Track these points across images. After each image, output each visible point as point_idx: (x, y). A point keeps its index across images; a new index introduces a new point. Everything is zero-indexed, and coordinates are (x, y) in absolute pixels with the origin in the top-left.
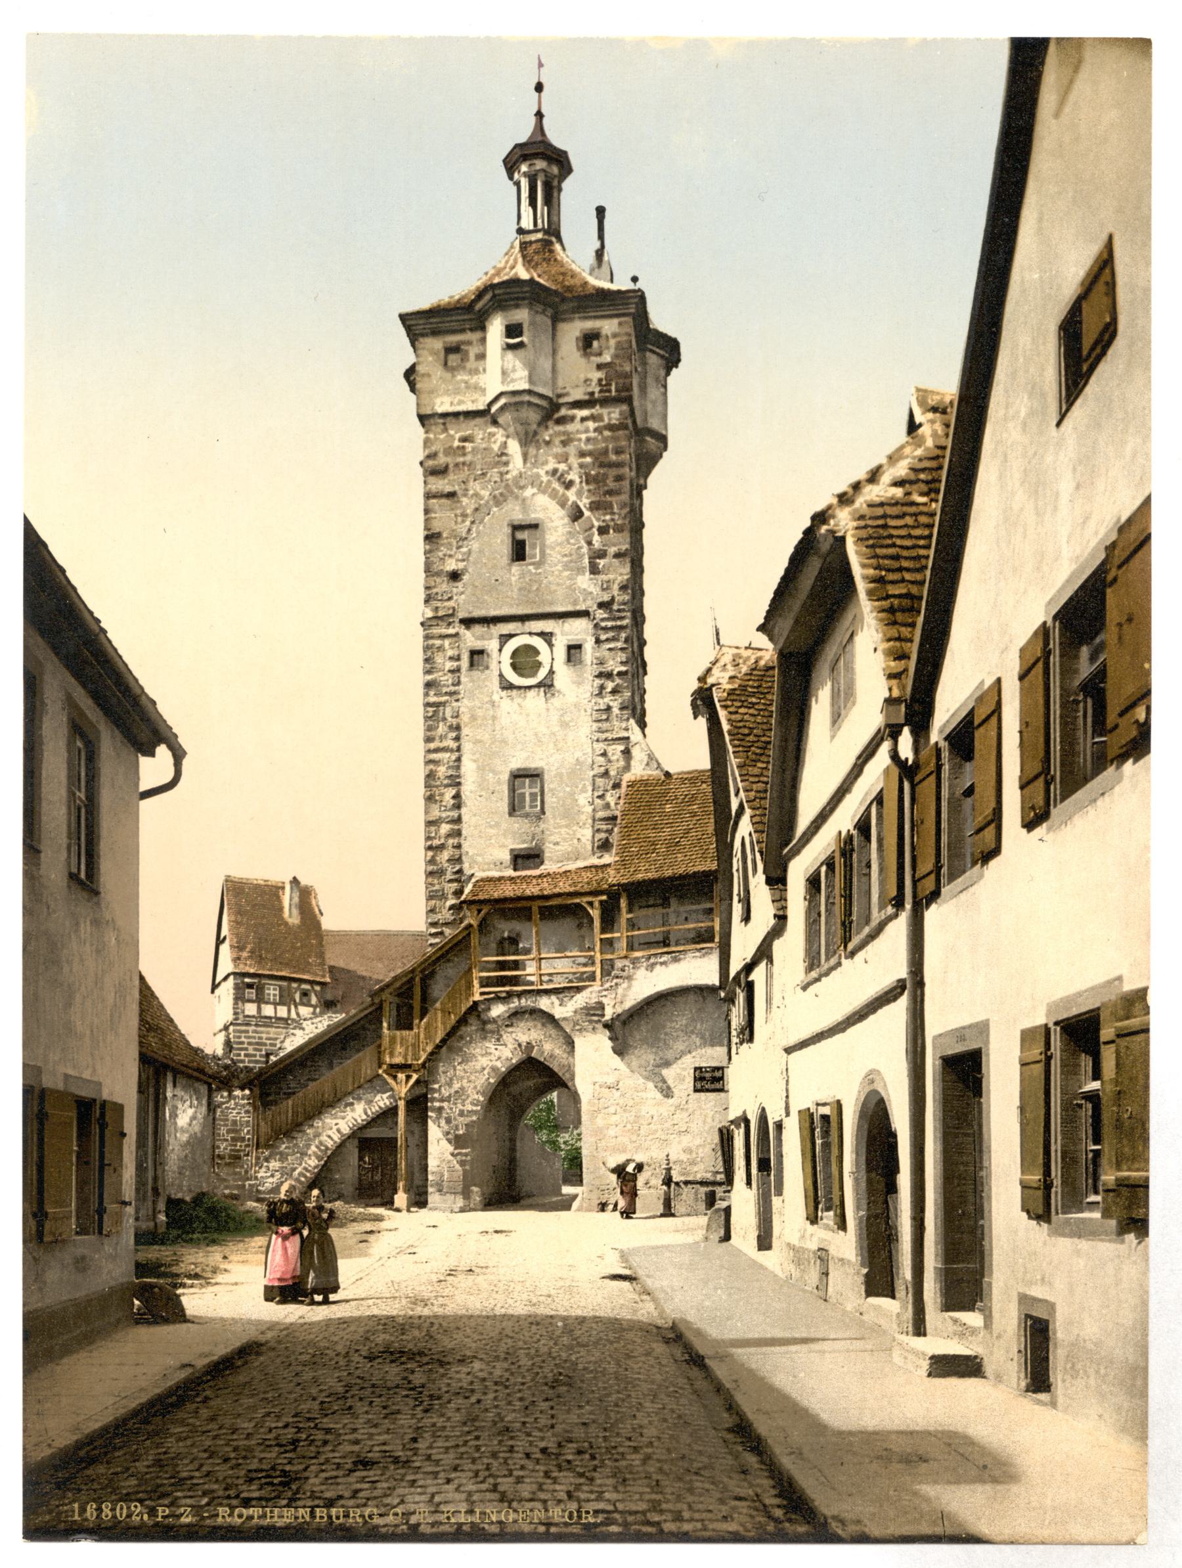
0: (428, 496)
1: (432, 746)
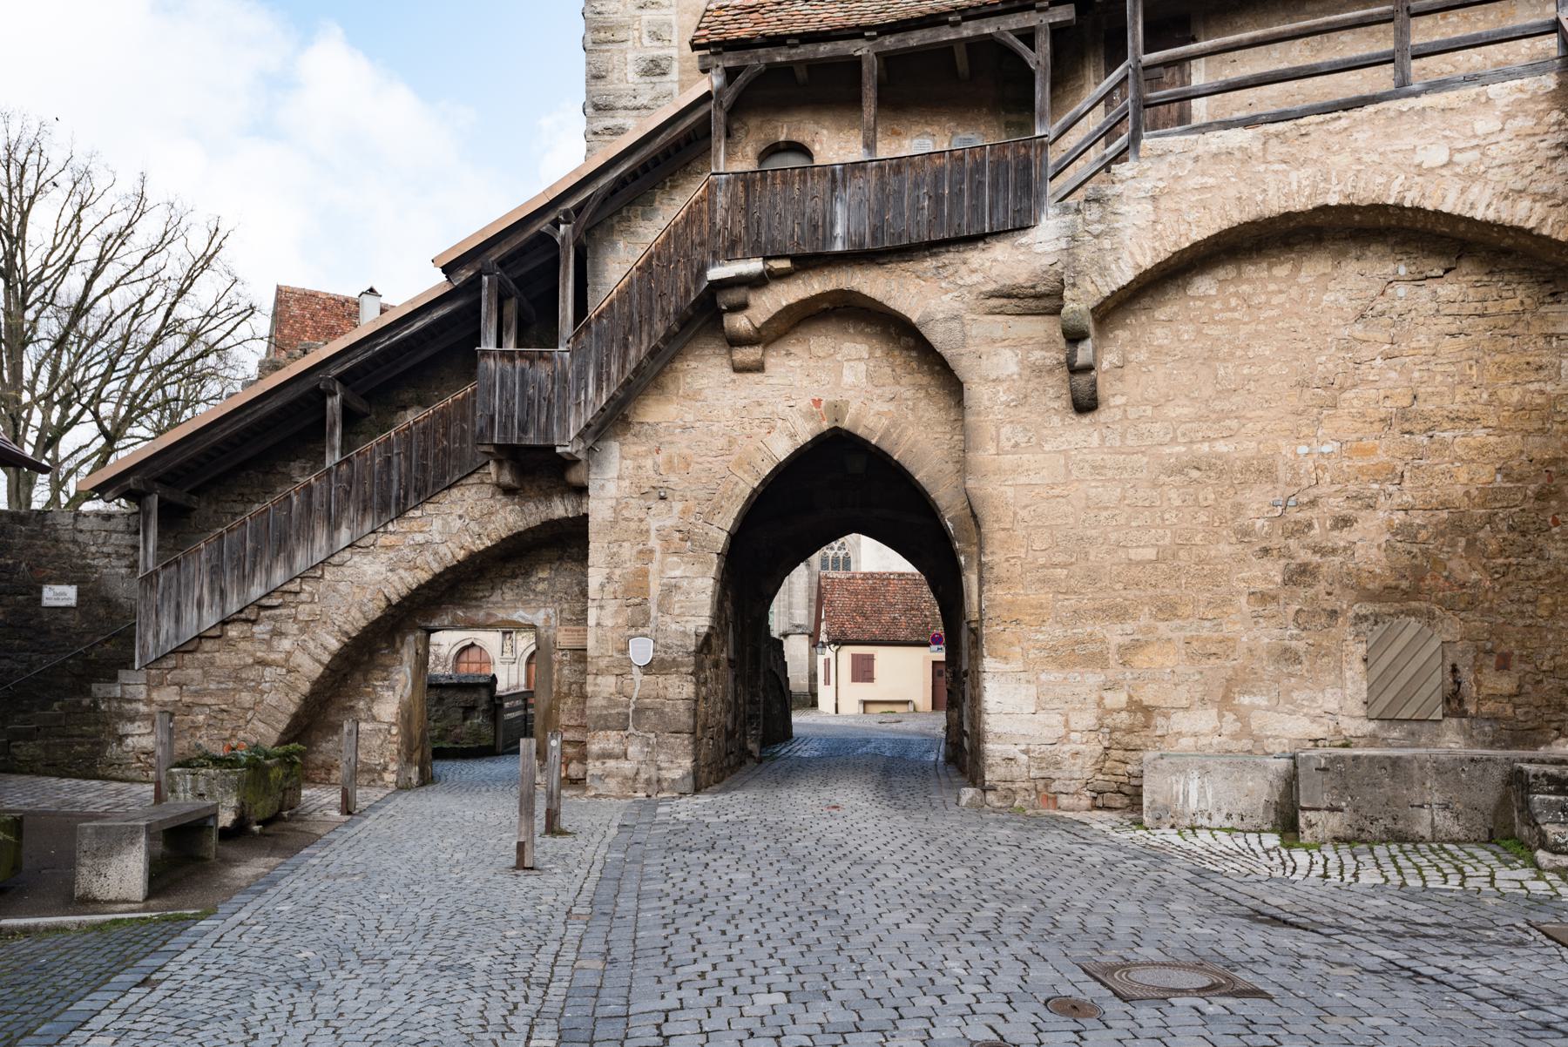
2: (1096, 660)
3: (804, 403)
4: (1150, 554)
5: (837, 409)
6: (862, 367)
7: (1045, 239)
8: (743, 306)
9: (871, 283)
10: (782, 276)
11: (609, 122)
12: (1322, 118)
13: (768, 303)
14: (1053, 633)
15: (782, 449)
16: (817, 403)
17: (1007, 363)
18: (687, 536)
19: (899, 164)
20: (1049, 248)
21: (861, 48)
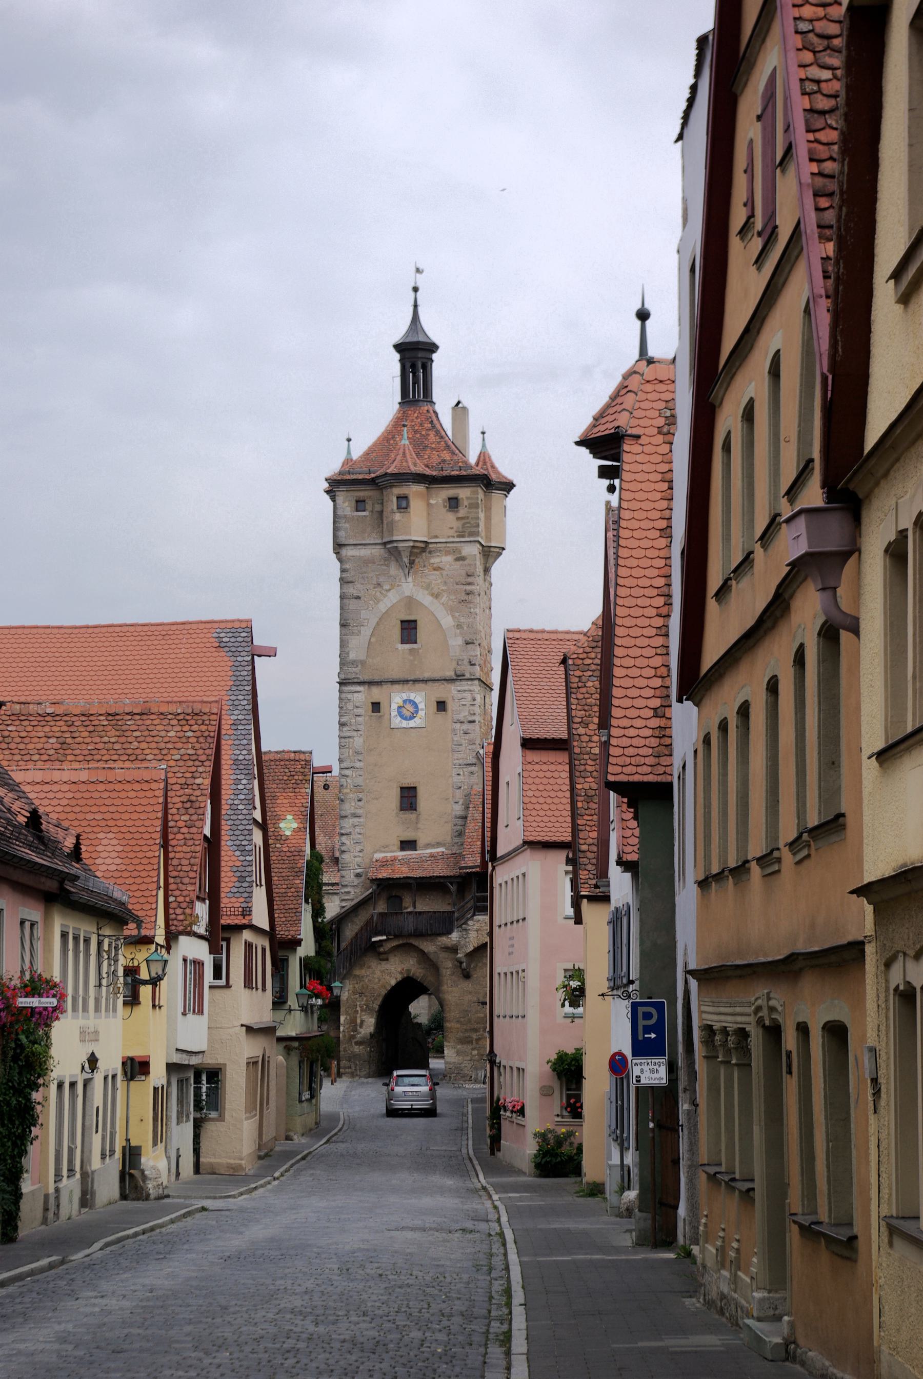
0: (342, 597)
1: (344, 765)
2: (470, 1042)
3: (399, 970)
5: (409, 971)
7: (455, 936)
8: (382, 946)
11: (346, 890)
13: (388, 946)
14: (460, 1035)
17: (449, 964)
18: (367, 1006)
19: (420, 913)
21: (410, 881)
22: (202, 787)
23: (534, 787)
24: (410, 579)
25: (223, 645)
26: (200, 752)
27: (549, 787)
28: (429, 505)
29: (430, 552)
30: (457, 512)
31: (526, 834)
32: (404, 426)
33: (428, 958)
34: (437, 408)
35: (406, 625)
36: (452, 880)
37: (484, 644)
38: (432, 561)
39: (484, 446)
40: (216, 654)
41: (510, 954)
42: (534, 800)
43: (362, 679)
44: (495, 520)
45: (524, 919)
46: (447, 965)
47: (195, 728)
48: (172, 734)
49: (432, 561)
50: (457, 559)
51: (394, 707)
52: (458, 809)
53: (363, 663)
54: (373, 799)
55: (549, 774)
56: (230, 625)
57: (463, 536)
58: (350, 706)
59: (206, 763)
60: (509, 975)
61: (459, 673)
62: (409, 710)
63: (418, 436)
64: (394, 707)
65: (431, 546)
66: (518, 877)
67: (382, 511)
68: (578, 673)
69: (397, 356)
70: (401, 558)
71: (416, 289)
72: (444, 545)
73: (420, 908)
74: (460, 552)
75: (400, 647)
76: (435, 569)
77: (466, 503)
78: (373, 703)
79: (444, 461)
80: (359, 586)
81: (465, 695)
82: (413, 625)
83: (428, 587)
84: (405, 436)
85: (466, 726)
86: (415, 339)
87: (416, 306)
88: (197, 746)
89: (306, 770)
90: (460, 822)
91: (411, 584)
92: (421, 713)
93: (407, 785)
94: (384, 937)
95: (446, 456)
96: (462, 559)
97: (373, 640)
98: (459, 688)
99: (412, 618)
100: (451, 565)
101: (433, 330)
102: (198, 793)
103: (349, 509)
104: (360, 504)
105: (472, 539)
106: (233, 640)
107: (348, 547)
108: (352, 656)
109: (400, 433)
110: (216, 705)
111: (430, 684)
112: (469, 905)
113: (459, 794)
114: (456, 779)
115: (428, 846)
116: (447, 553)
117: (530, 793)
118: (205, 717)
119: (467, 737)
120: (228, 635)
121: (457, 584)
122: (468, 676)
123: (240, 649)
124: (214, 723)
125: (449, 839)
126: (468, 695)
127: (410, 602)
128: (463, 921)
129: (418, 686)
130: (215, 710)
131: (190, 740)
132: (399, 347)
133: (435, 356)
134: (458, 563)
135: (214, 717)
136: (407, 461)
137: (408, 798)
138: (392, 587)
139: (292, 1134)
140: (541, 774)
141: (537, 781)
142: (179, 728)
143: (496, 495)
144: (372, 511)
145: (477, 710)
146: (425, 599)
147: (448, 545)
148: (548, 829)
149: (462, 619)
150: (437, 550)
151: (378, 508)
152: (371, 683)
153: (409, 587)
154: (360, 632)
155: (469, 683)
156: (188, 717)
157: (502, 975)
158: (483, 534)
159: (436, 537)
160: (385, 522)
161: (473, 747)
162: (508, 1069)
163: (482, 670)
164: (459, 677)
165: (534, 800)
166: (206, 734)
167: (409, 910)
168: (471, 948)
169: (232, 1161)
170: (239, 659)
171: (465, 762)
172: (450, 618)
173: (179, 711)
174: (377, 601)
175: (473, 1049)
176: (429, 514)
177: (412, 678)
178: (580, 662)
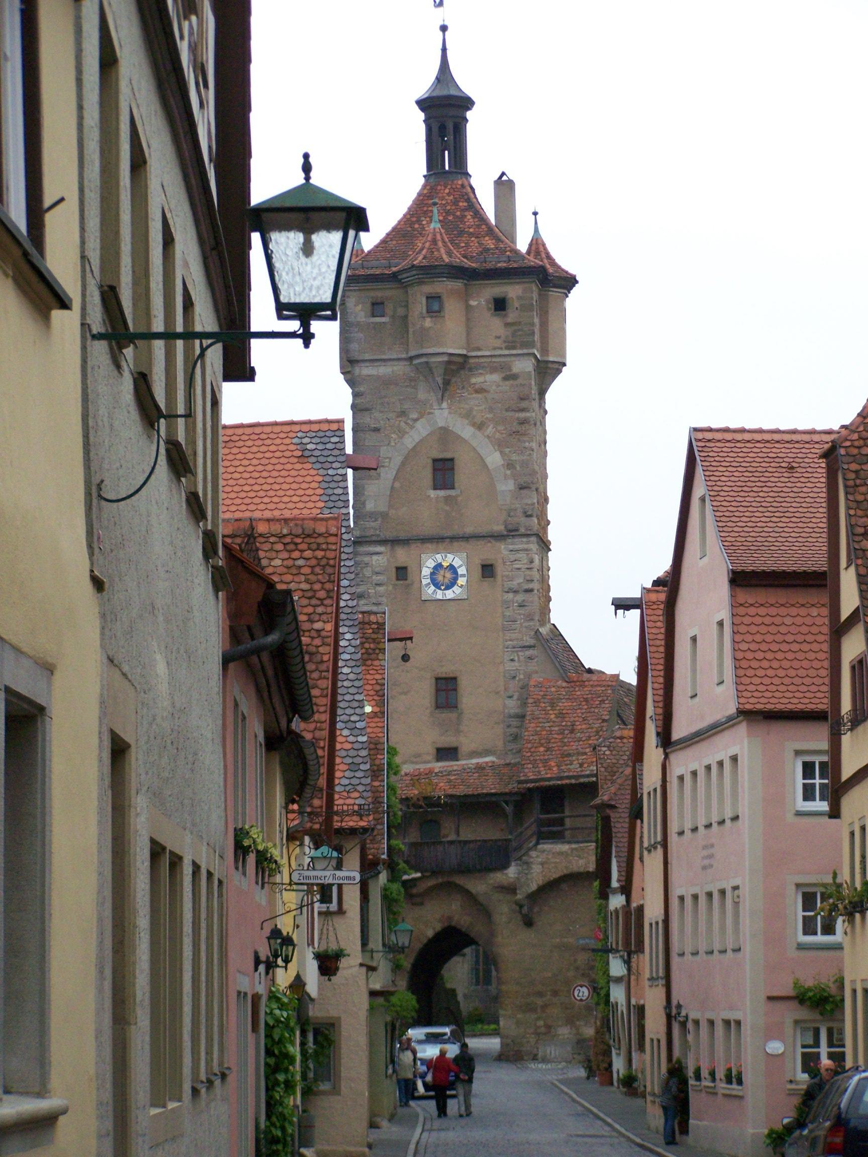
4: (550, 975)
5: (450, 918)
6: (459, 903)
7: (512, 872)
8: (415, 886)
9: (460, 880)
10: (427, 877)
12: (586, 844)
15: (430, 933)
16: (443, 916)
20: (512, 876)
22: (323, 634)
23: (749, 638)
24: (445, 405)
25: (307, 453)
26: (317, 586)
27: (769, 638)
28: (468, 308)
29: (470, 370)
30: (505, 316)
31: (742, 700)
32: (435, 204)
33: (476, 900)
34: (474, 182)
35: (439, 465)
36: (507, 798)
37: (541, 489)
38: (473, 380)
39: (536, 230)
40: (298, 466)
41: (704, 868)
42: (749, 655)
43: (382, 537)
44: (553, 327)
45: (736, 818)
46: (503, 911)
47: (308, 554)
48: (277, 562)
49: (473, 380)
50: (506, 379)
51: (426, 572)
52: (512, 706)
53: (384, 516)
54: (401, 694)
55: (767, 620)
56: (315, 427)
57: (514, 348)
58: (367, 572)
59: (327, 602)
60: (702, 900)
61: (510, 527)
62: (445, 577)
63: (451, 218)
64: (426, 572)
65: (472, 361)
66: (721, 764)
67: (406, 317)
68: (854, 467)
69: (421, 116)
70: (434, 378)
71: (444, 28)
72: (489, 360)
73: (467, 834)
74: (510, 370)
75: (433, 494)
76: (477, 392)
77: (517, 304)
78: (398, 569)
79: (487, 250)
80: (377, 414)
81: (518, 556)
82: (448, 464)
83: (467, 414)
84: (436, 217)
85: (520, 597)
86: (445, 92)
87: (444, 50)
88: (313, 578)
89: (380, 636)
90: (515, 722)
91: (446, 412)
92: (462, 581)
93: (444, 676)
94: (419, 875)
95: (490, 243)
96: (514, 377)
97: (397, 485)
98: (511, 547)
99: (448, 455)
100: (498, 386)
101: (466, 81)
102: (317, 642)
103: (363, 314)
104: (377, 307)
105: (525, 351)
106: (320, 447)
107: (360, 364)
108: (370, 506)
109: (428, 214)
110: (335, 523)
111: (473, 542)
112: (529, 832)
113: (513, 686)
114: (509, 666)
115: (474, 754)
116: (493, 370)
117: (744, 646)
118: (321, 540)
119: (522, 611)
120: (314, 441)
121: (507, 410)
122: (522, 530)
123: (330, 459)
124: (334, 547)
125: (500, 744)
126: (522, 556)
127: (445, 435)
128: (523, 852)
129: (456, 544)
130: (333, 530)
131: (303, 571)
132: (424, 104)
133: (469, 115)
134: (507, 383)
135: (332, 539)
136: (438, 250)
137: (446, 690)
138: (421, 415)
139: (378, 1120)
140: (758, 620)
141: (754, 629)
142: (285, 555)
143: (554, 293)
144: (393, 317)
145: (536, 575)
146: (466, 432)
147: (494, 360)
148: (770, 695)
149: (514, 457)
150: (479, 366)
151: (401, 311)
152: (395, 542)
153: (443, 415)
154: (379, 474)
155: (524, 540)
156: (299, 540)
157: (689, 901)
158: (538, 345)
159: (479, 349)
160: (411, 330)
161: (531, 623)
162: (704, 1027)
163: (539, 524)
164: (511, 533)
165: (749, 655)
166: (324, 562)
167: (449, 839)
168: (534, 887)
169: (352, 1149)
170: (331, 472)
171: (521, 643)
172: (497, 455)
173: (285, 531)
174: (402, 433)
175: (538, 1019)
176: (468, 320)
177: (449, 534)
178: (855, 451)
